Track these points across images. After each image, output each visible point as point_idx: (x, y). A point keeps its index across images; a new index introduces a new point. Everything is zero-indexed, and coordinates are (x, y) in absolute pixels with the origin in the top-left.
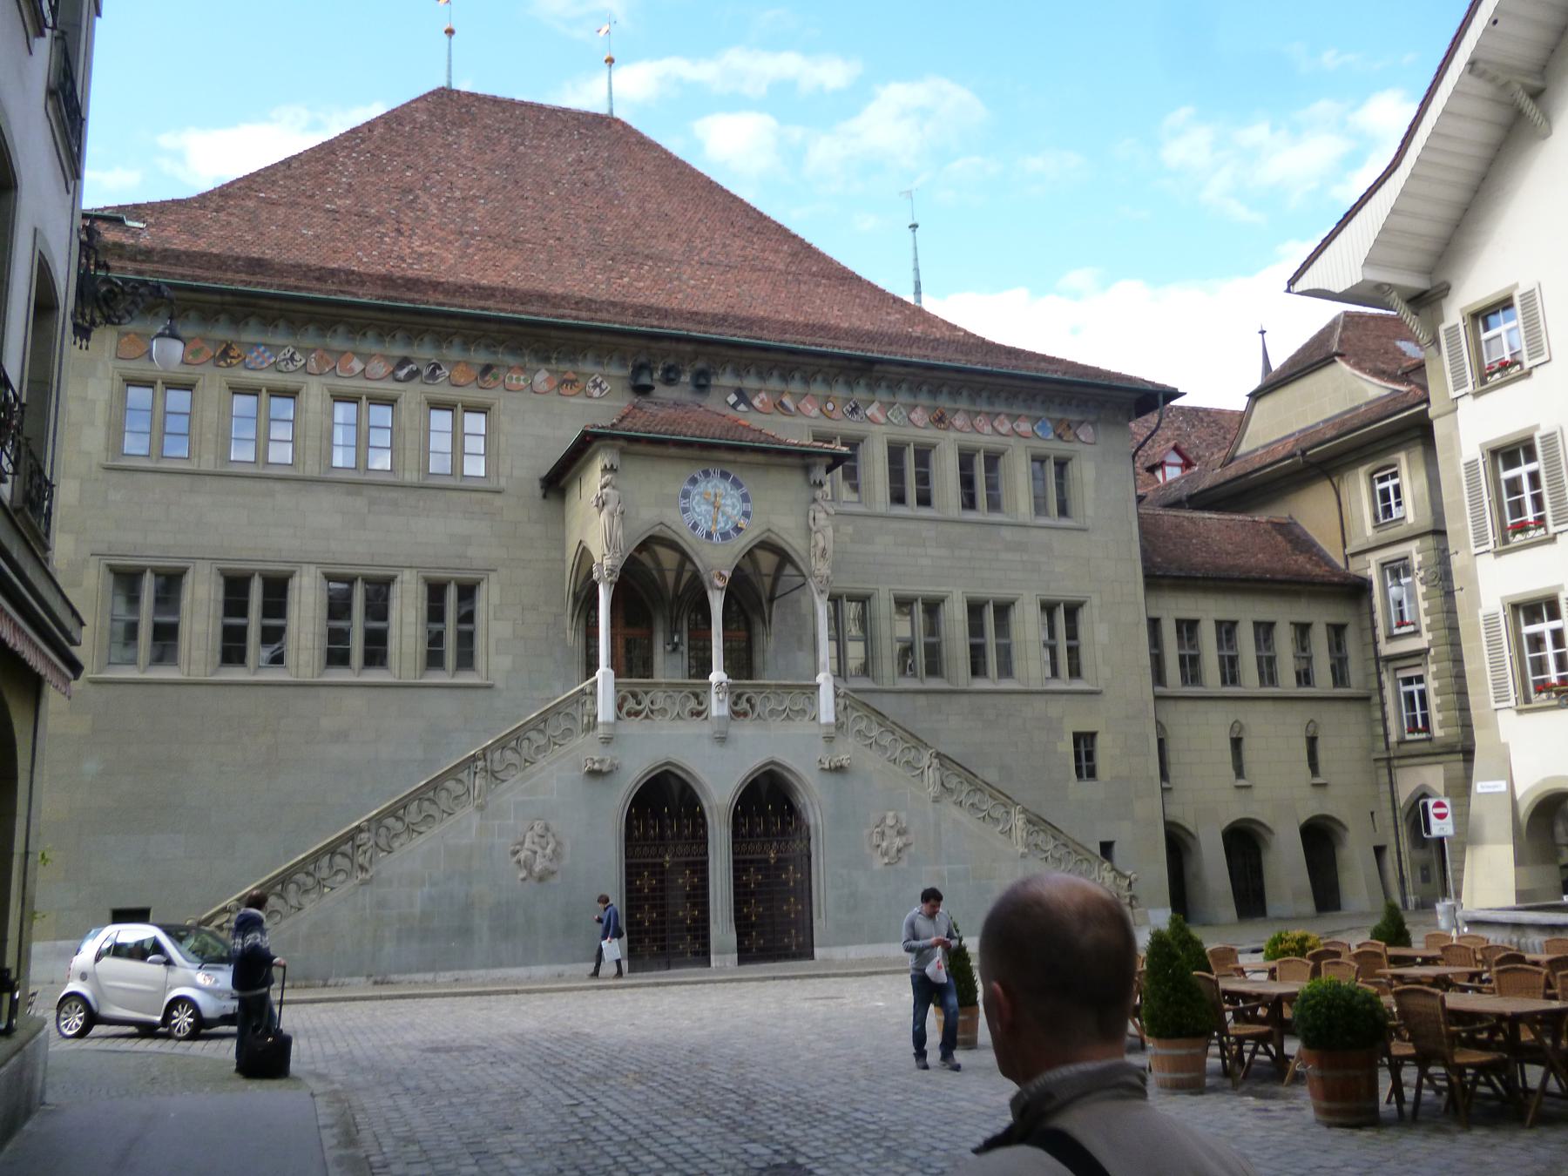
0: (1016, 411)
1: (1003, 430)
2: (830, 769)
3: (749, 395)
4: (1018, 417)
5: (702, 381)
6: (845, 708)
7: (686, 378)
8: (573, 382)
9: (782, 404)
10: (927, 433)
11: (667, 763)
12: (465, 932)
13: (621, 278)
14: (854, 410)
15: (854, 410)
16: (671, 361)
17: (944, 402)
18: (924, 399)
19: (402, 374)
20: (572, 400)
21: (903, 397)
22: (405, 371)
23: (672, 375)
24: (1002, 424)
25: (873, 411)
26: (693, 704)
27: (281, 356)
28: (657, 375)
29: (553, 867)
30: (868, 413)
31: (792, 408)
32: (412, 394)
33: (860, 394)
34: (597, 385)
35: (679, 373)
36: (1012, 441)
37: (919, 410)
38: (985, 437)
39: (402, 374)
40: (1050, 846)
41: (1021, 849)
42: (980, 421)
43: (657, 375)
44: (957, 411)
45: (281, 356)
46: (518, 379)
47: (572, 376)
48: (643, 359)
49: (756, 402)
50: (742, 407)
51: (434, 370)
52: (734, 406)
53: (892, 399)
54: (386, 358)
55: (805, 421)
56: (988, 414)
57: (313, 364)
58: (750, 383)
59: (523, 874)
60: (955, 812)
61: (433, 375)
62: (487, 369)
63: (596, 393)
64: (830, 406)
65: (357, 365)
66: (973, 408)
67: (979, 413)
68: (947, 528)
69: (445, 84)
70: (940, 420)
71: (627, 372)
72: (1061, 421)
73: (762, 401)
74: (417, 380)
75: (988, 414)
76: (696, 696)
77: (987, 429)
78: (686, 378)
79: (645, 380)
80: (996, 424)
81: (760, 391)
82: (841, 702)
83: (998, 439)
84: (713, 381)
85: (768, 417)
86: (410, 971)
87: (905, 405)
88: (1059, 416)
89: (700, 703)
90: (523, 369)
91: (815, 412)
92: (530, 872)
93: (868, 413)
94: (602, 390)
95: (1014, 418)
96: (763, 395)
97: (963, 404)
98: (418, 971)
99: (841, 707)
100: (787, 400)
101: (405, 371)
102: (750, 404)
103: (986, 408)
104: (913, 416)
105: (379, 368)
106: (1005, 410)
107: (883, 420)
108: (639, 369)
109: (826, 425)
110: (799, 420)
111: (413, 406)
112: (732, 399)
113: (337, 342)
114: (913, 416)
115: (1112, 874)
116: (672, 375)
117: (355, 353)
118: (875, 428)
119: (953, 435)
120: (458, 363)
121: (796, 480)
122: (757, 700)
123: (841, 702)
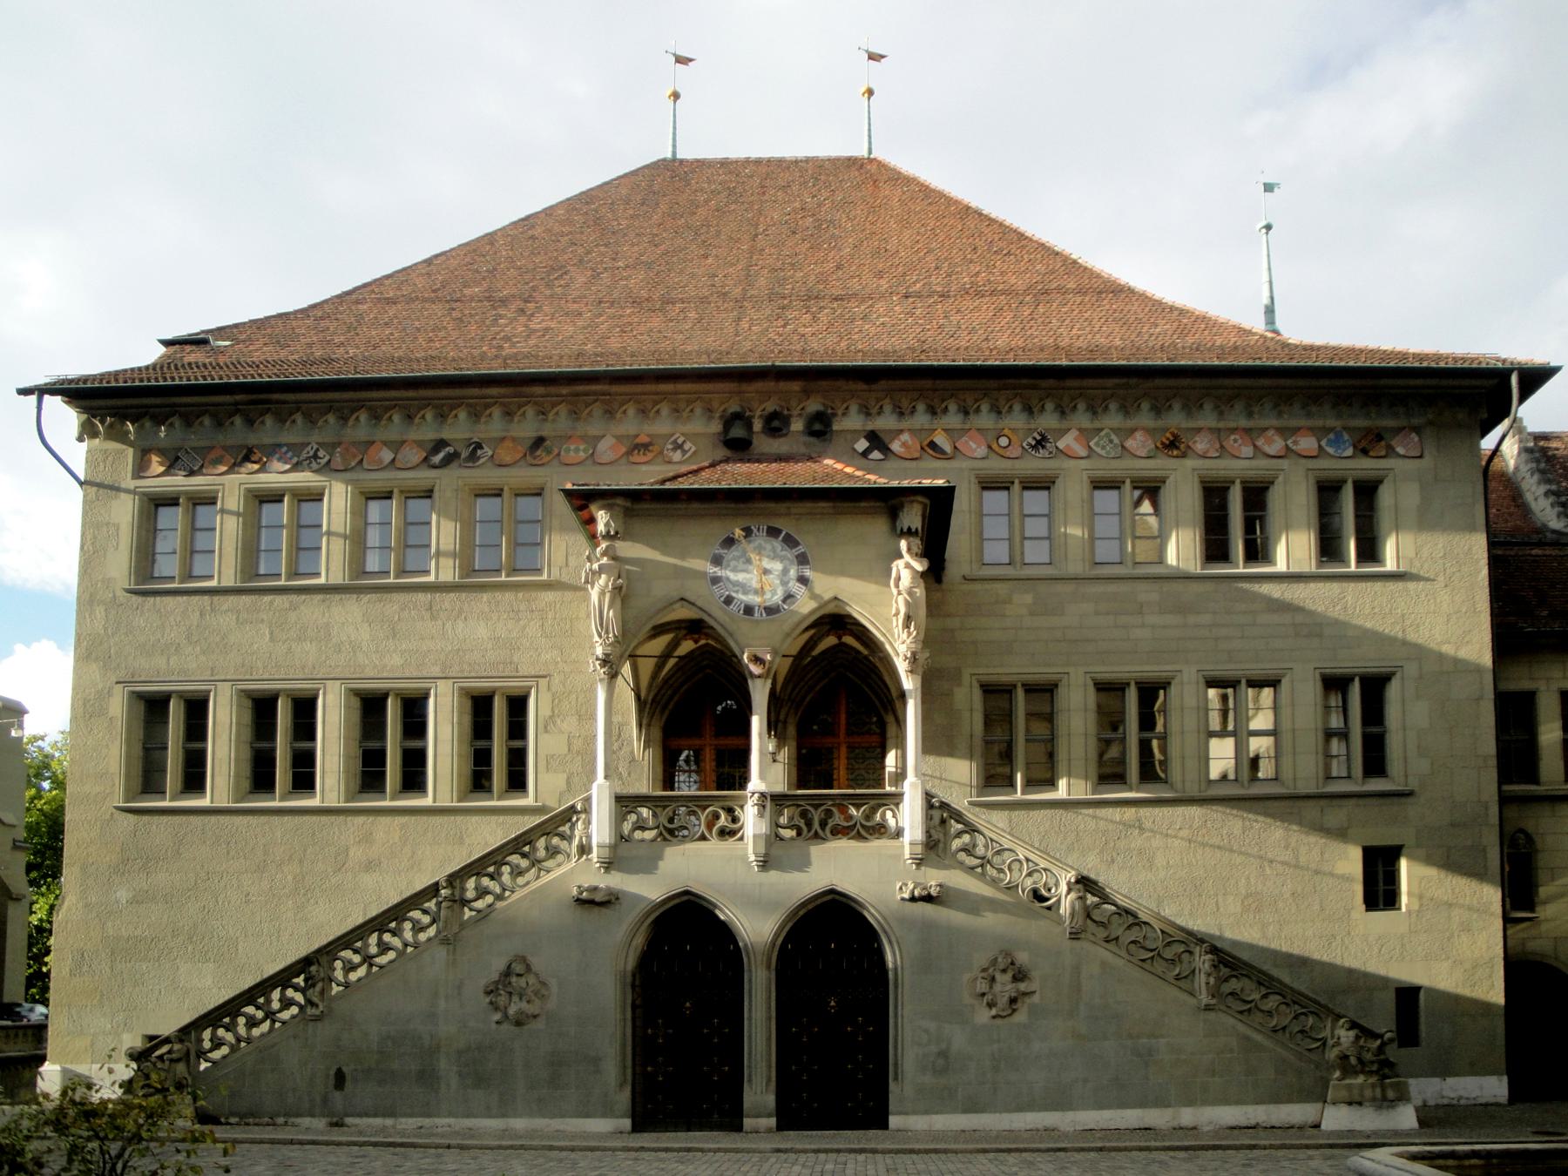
0: (1294, 423)
1: (1271, 450)
2: (913, 899)
3: (886, 439)
4: (1295, 431)
5: (817, 427)
6: (943, 821)
7: (797, 425)
8: (646, 447)
9: (933, 445)
10: (1151, 463)
11: (687, 893)
12: (427, 1077)
13: (784, 326)
14: (1041, 443)
15: (1041, 443)
16: (771, 406)
17: (1176, 420)
18: (1145, 419)
19: (437, 459)
20: (644, 468)
21: (1113, 420)
22: (441, 455)
23: (776, 424)
24: (1270, 442)
25: (1068, 441)
26: (723, 820)
27: (304, 455)
28: (758, 425)
29: (531, 1009)
30: (1061, 445)
31: (948, 448)
32: (449, 481)
33: (1048, 420)
34: (678, 447)
35: (786, 421)
36: (1284, 464)
37: (1139, 435)
38: (1240, 463)
39: (437, 459)
40: (1256, 996)
41: (1205, 998)
42: (1232, 442)
43: (758, 425)
44: (1199, 430)
45: (304, 455)
46: (577, 450)
47: (643, 439)
48: (734, 408)
49: (896, 446)
50: (876, 455)
51: (475, 450)
52: (865, 454)
53: (1097, 424)
54: (420, 444)
55: (965, 464)
56: (1248, 431)
57: (338, 461)
58: (885, 422)
59: (497, 1016)
60: (1103, 953)
61: (473, 457)
62: (539, 442)
63: (677, 456)
64: (1004, 441)
65: (387, 456)
66: (1221, 425)
67: (1233, 430)
68: (1177, 587)
69: (669, 155)
70: (1173, 445)
71: (716, 427)
72: (1368, 431)
73: (904, 444)
74: (455, 464)
75: (1248, 431)
76: (730, 811)
77: (1247, 451)
78: (797, 425)
79: (737, 432)
80: (1260, 443)
81: (902, 431)
82: (936, 814)
83: (1263, 463)
84: (835, 427)
85: (914, 463)
86: (367, 1115)
87: (1115, 430)
88: (1360, 423)
89: (735, 820)
90: (584, 438)
91: (981, 451)
92: (506, 1016)
93: (1061, 445)
94: (685, 452)
95: (1285, 432)
96: (905, 437)
97: (1207, 419)
98: (376, 1115)
99: (937, 820)
100: (941, 440)
101: (441, 455)
102: (885, 450)
103: (1243, 423)
104: (1129, 443)
105: (413, 455)
106: (1275, 422)
107: (1083, 453)
108: (730, 421)
109: (997, 466)
110: (954, 464)
111: (448, 494)
112: (862, 445)
113: (361, 426)
114: (1129, 443)
115: (1352, 1034)
116: (776, 424)
117: (385, 443)
118: (1073, 462)
119: (1190, 463)
120: (503, 439)
121: (877, 527)
122: (817, 816)
123: (936, 814)
